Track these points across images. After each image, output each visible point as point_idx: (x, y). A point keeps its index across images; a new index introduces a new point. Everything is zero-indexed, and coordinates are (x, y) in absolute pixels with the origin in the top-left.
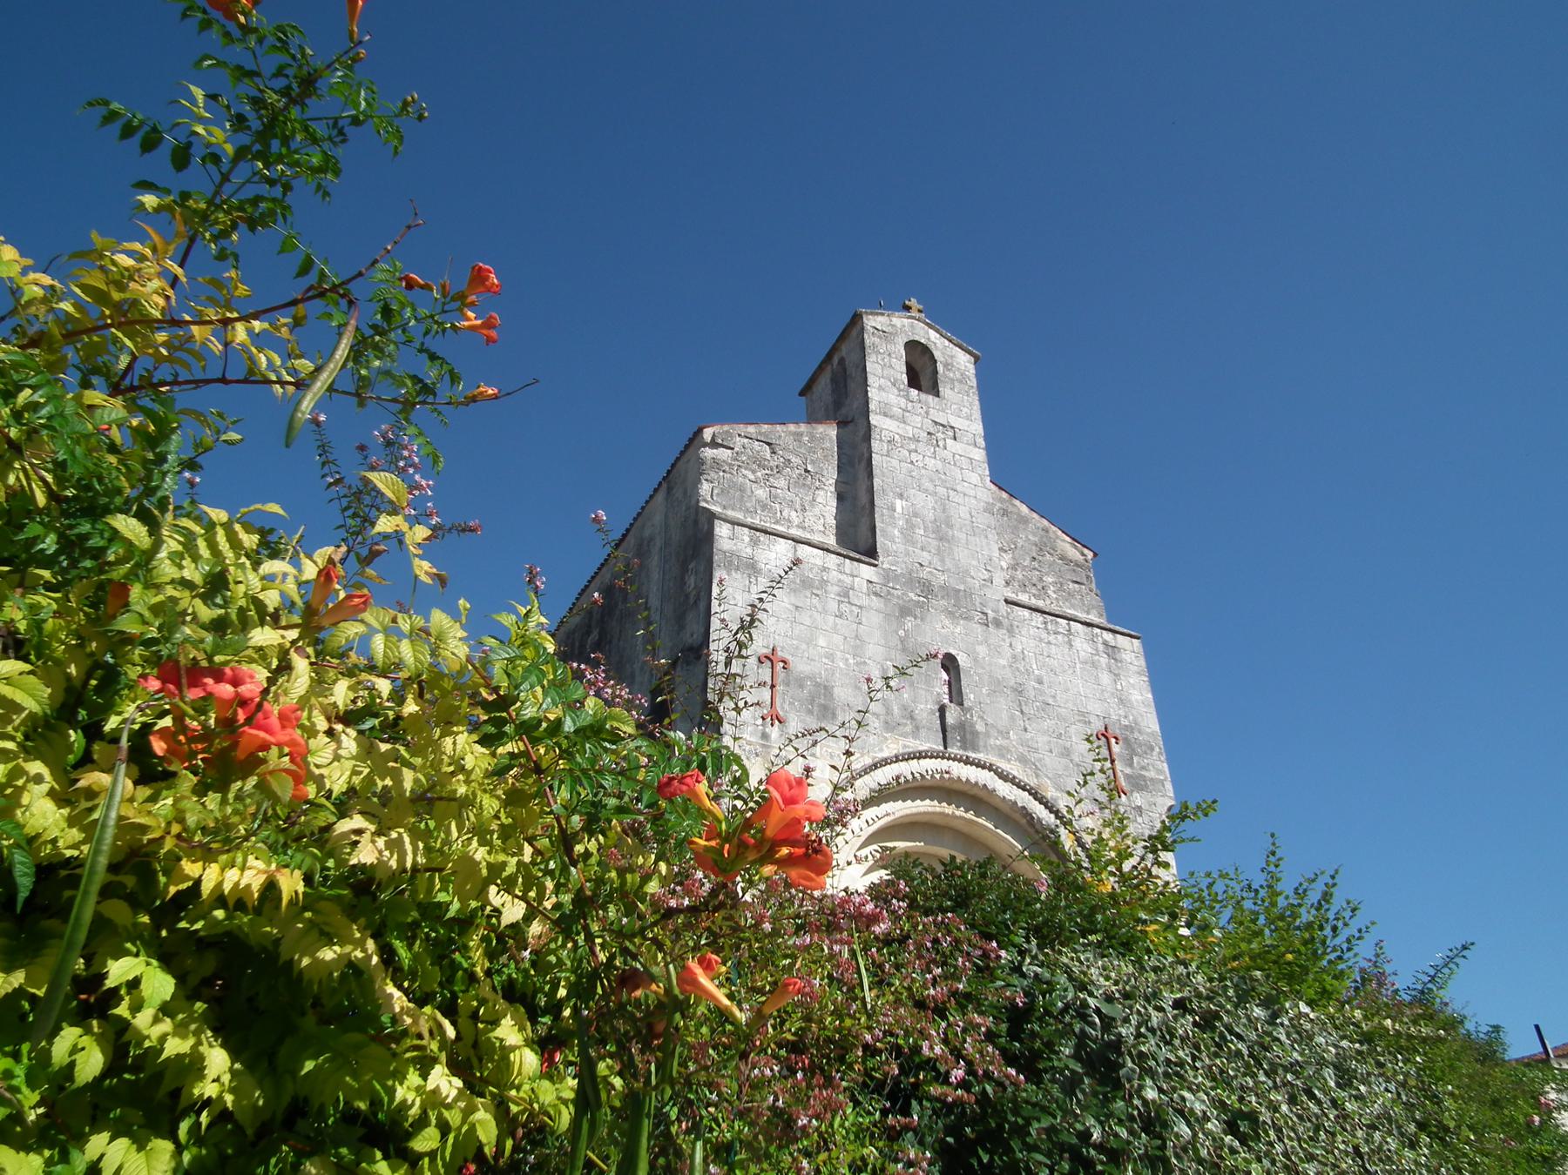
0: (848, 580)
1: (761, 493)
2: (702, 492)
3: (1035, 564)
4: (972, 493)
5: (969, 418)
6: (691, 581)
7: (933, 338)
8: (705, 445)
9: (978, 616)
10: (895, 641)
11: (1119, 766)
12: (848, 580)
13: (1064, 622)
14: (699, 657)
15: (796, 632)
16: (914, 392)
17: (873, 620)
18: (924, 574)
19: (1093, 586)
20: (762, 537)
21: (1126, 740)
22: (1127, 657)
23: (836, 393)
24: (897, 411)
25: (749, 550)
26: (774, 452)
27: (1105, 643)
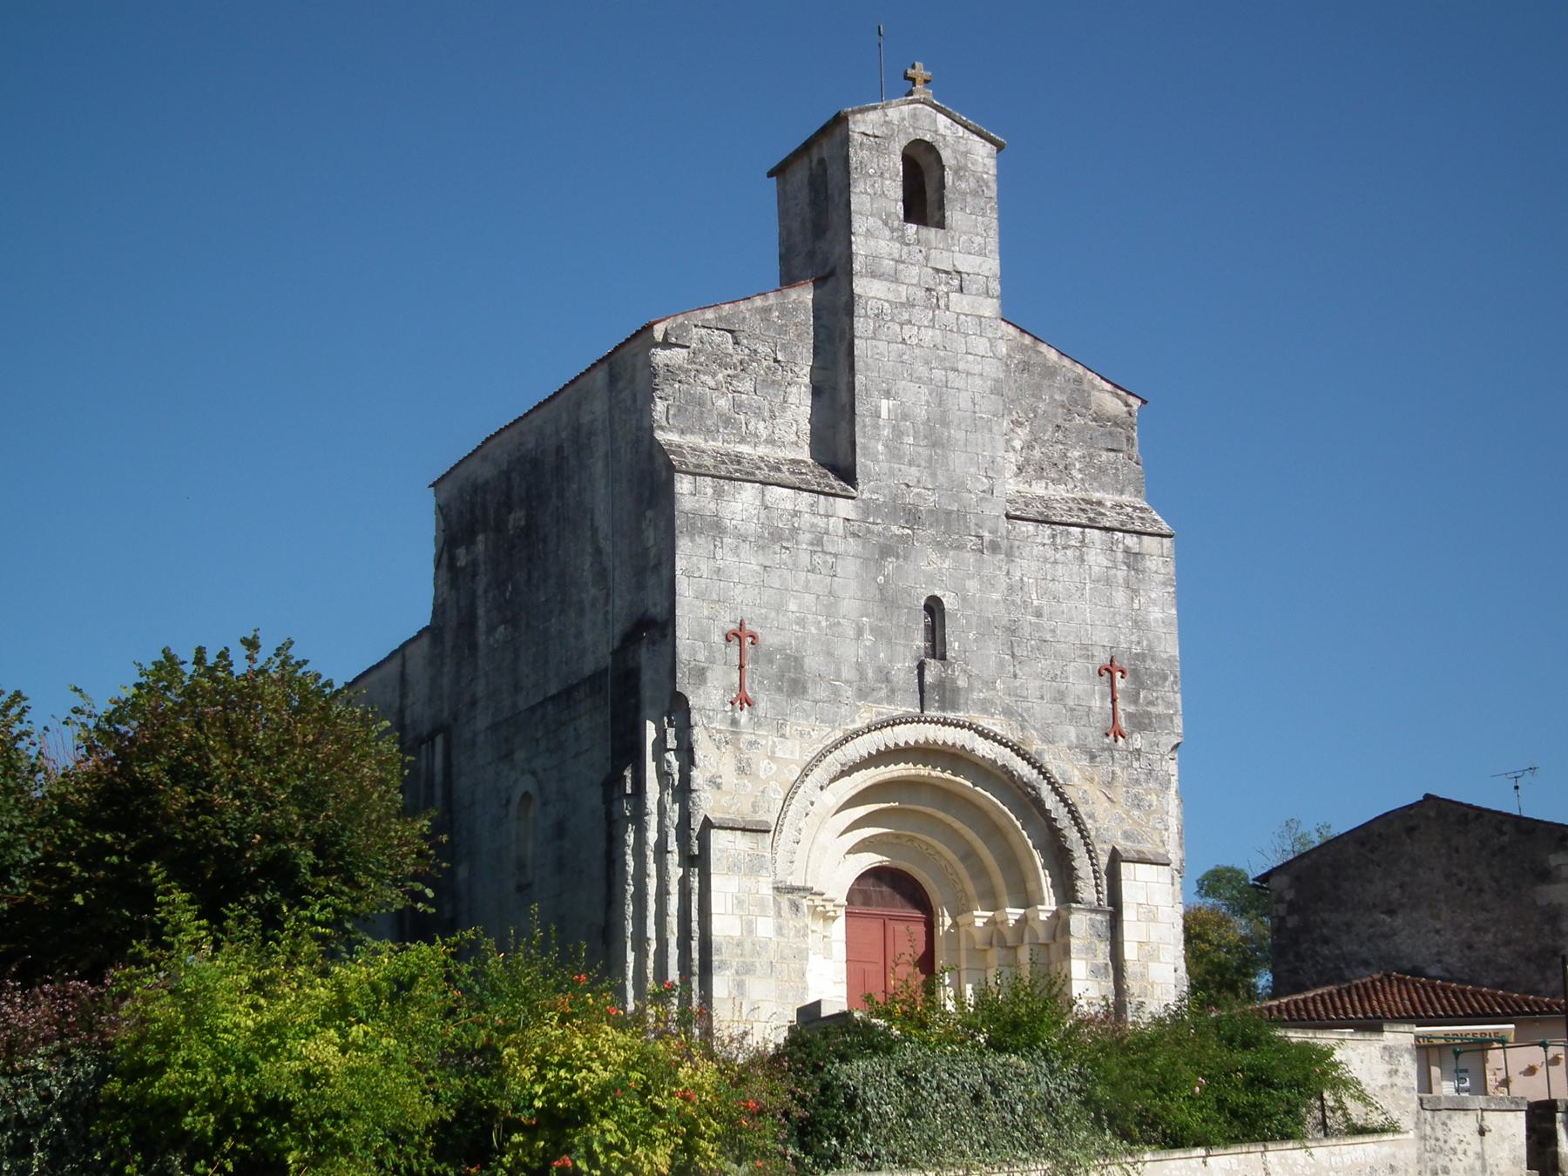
0: (821, 522)
1: (723, 403)
2: (656, 415)
3: (1059, 435)
4: (977, 369)
5: (982, 253)
6: (650, 536)
7: (943, 130)
8: (657, 345)
9: (971, 542)
10: (873, 591)
11: (1120, 705)
12: (821, 522)
13: (1077, 530)
14: (664, 636)
15: (765, 598)
16: (912, 228)
17: (849, 568)
18: (909, 499)
19: (1135, 451)
20: (727, 486)
21: (1135, 672)
22: (1152, 564)
23: (816, 249)
24: (888, 264)
25: (712, 506)
26: (736, 343)
27: (1127, 551)
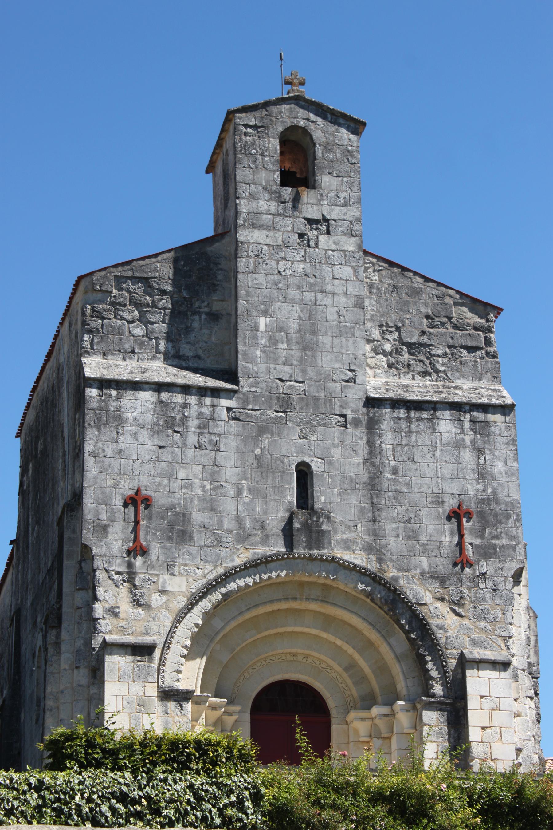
10: (251, 461)
11: (467, 539)
15: (159, 471)
17: (230, 445)
21: (482, 515)
